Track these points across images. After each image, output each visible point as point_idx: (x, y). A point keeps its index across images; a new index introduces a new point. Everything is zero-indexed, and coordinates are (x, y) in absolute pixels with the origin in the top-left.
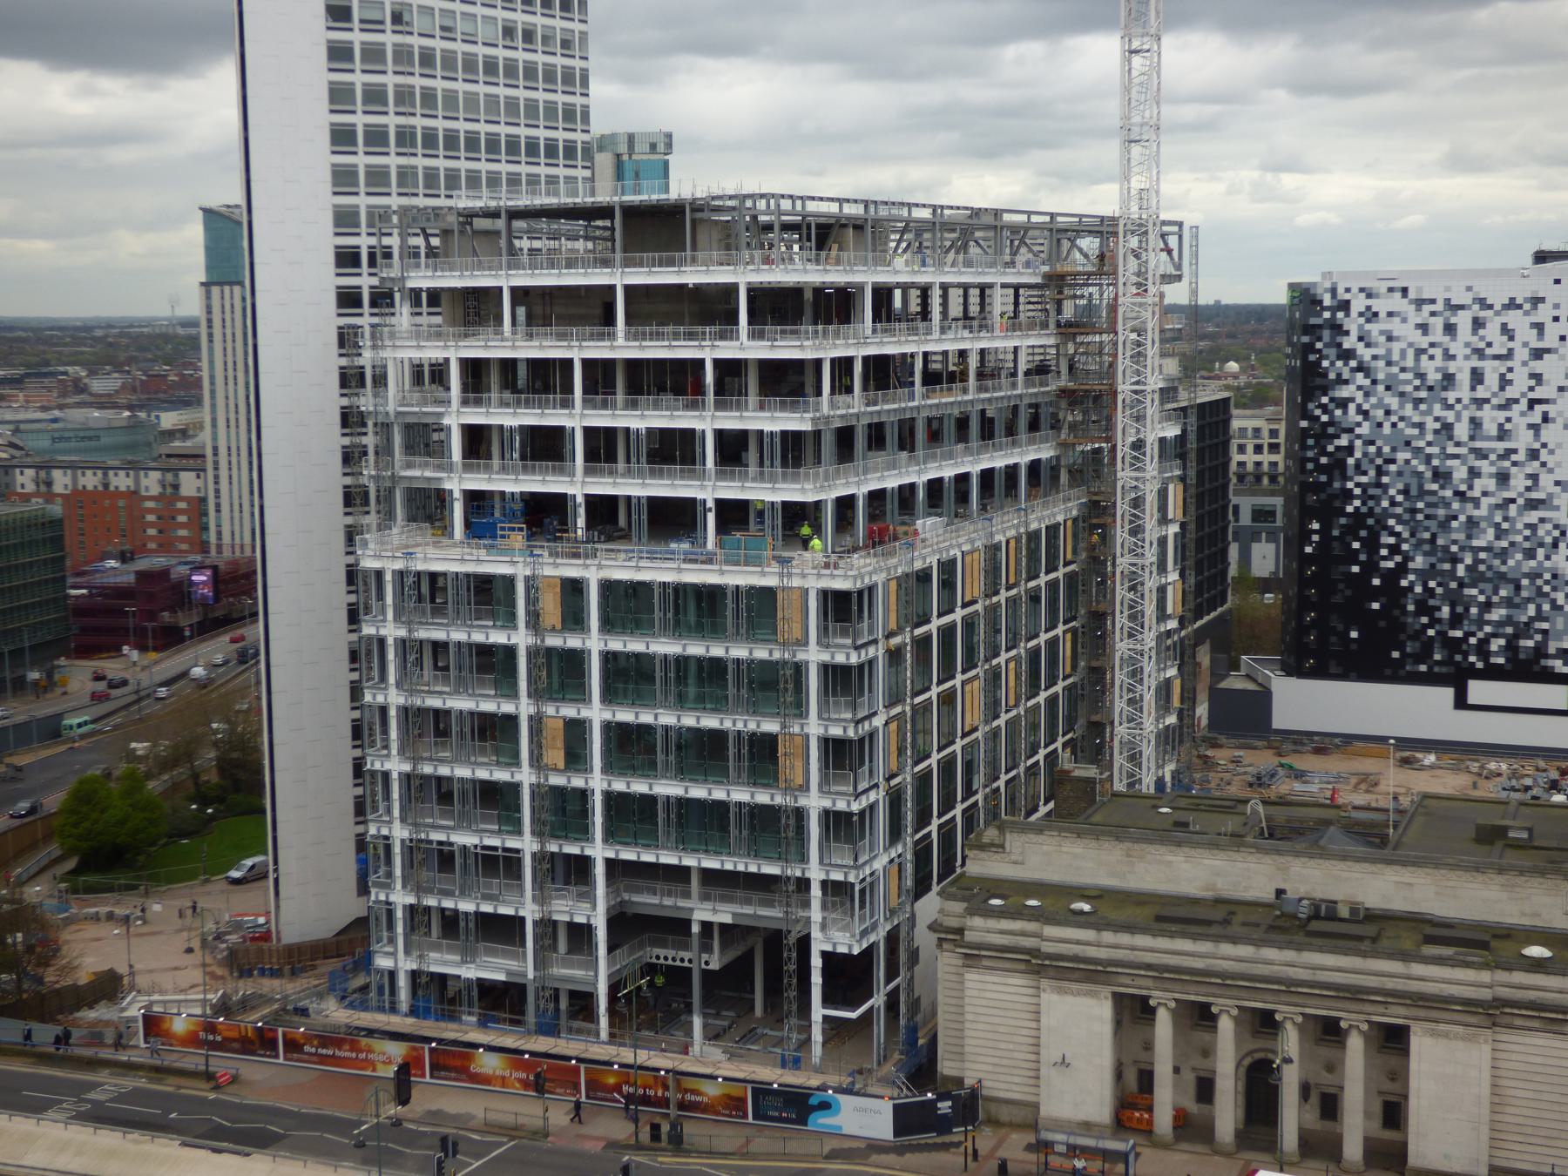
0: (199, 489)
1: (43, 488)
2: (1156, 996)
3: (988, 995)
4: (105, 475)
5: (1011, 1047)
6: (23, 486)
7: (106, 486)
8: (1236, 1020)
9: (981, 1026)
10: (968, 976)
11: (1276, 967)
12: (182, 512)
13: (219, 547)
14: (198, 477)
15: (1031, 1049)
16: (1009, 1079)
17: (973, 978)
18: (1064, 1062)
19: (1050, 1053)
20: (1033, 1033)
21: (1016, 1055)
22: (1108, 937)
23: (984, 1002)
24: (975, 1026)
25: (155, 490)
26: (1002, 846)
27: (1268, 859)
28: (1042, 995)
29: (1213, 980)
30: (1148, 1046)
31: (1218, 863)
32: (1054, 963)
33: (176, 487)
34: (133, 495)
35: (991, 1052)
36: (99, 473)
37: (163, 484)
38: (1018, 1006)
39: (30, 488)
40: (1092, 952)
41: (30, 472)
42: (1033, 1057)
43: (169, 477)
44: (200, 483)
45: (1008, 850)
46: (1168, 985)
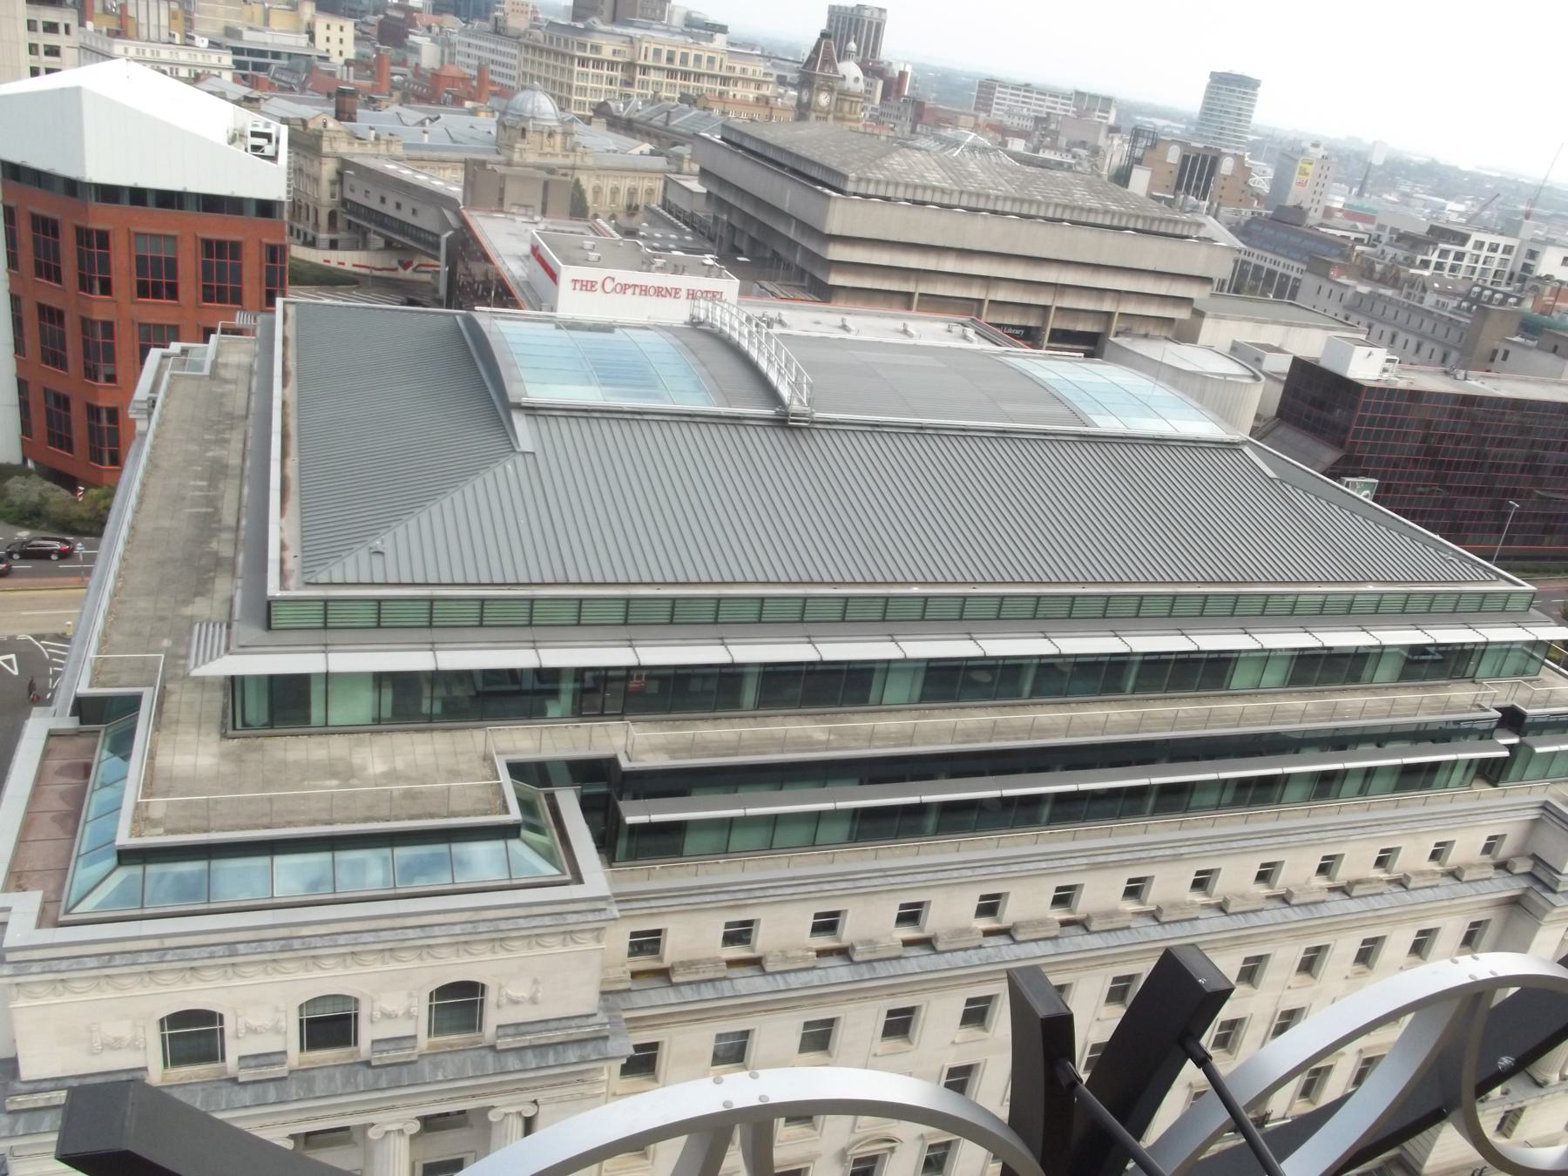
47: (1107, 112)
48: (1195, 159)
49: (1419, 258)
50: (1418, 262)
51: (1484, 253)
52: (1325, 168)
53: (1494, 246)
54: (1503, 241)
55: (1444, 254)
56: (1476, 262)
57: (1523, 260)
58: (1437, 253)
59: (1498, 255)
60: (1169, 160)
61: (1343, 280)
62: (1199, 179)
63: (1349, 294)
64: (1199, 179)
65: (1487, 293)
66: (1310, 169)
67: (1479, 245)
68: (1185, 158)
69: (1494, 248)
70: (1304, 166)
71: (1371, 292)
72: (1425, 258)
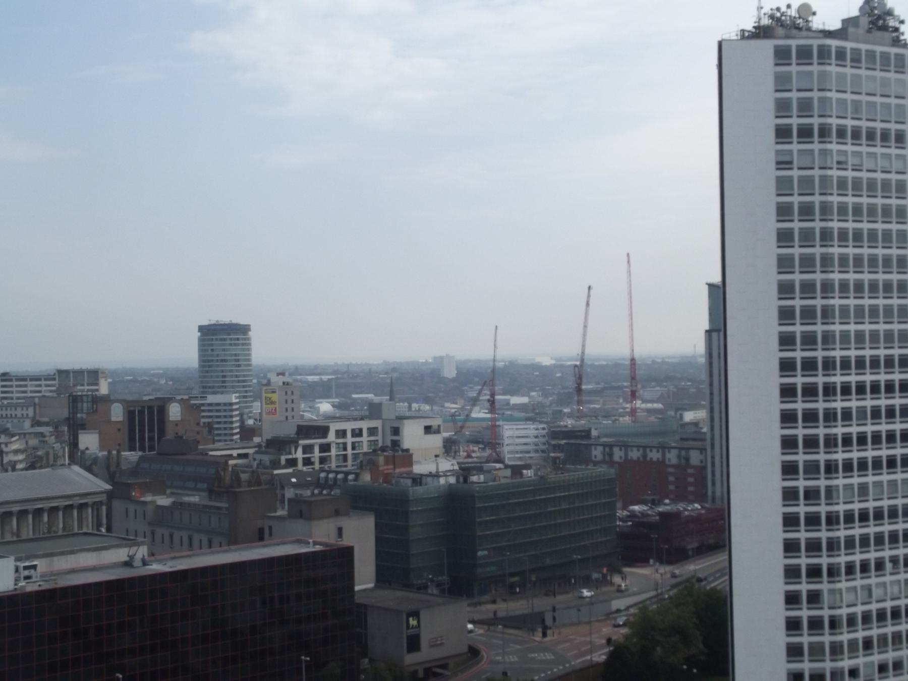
0: (702, 462)
1: (607, 458)
4: (645, 451)
6: (595, 456)
7: (645, 456)
12: (691, 475)
13: (714, 498)
14: (701, 453)
25: (674, 461)
33: (687, 459)
34: (662, 463)
36: (641, 449)
37: (679, 457)
39: (600, 457)
41: (600, 449)
43: (683, 453)
44: (702, 457)
47: (97, 384)
48: (141, 412)
49: (283, 459)
50: (283, 462)
51: (349, 439)
52: (289, 393)
53: (357, 431)
54: (364, 425)
55: (308, 449)
56: (345, 449)
57: (390, 438)
58: (300, 450)
59: (365, 438)
60: (114, 419)
61: (148, 498)
62: (151, 430)
63: (150, 509)
64: (151, 430)
65: (331, 476)
66: (275, 397)
67: (341, 434)
68: (130, 414)
69: (357, 433)
70: (270, 395)
71: (174, 503)
72: (290, 457)
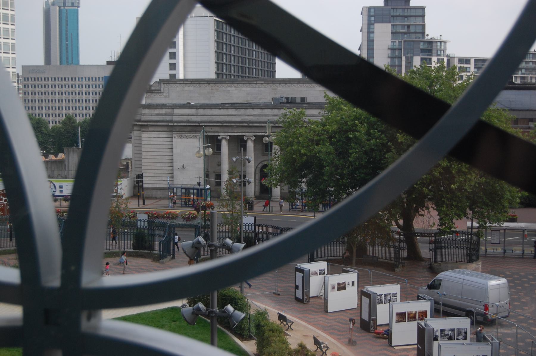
2: (221, 135)
3: (152, 143)
5: (162, 164)
8: (255, 142)
9: (148, 157)
10: (143, 135)
11: (270, 117)
15: (170, 165)
16: (160, 179)
17: (145, 136)
18: (183, 167)
19: (177, 164)
20: (170, 158)
21: (163, 168)
22: (201, 111)
23: (150, 146)
24: (146, 157)
26: (160, 90)
27: (268, 86)
28: (174, 140)
29: (244, 125)
30: (219, 165)
31: (249, 89)
32: (179, 124)
35: (153, 168)
38: (164, 147)
40: (194, 118)
42: (171, 168)
45: (162, 91)
46: (226, 129)
